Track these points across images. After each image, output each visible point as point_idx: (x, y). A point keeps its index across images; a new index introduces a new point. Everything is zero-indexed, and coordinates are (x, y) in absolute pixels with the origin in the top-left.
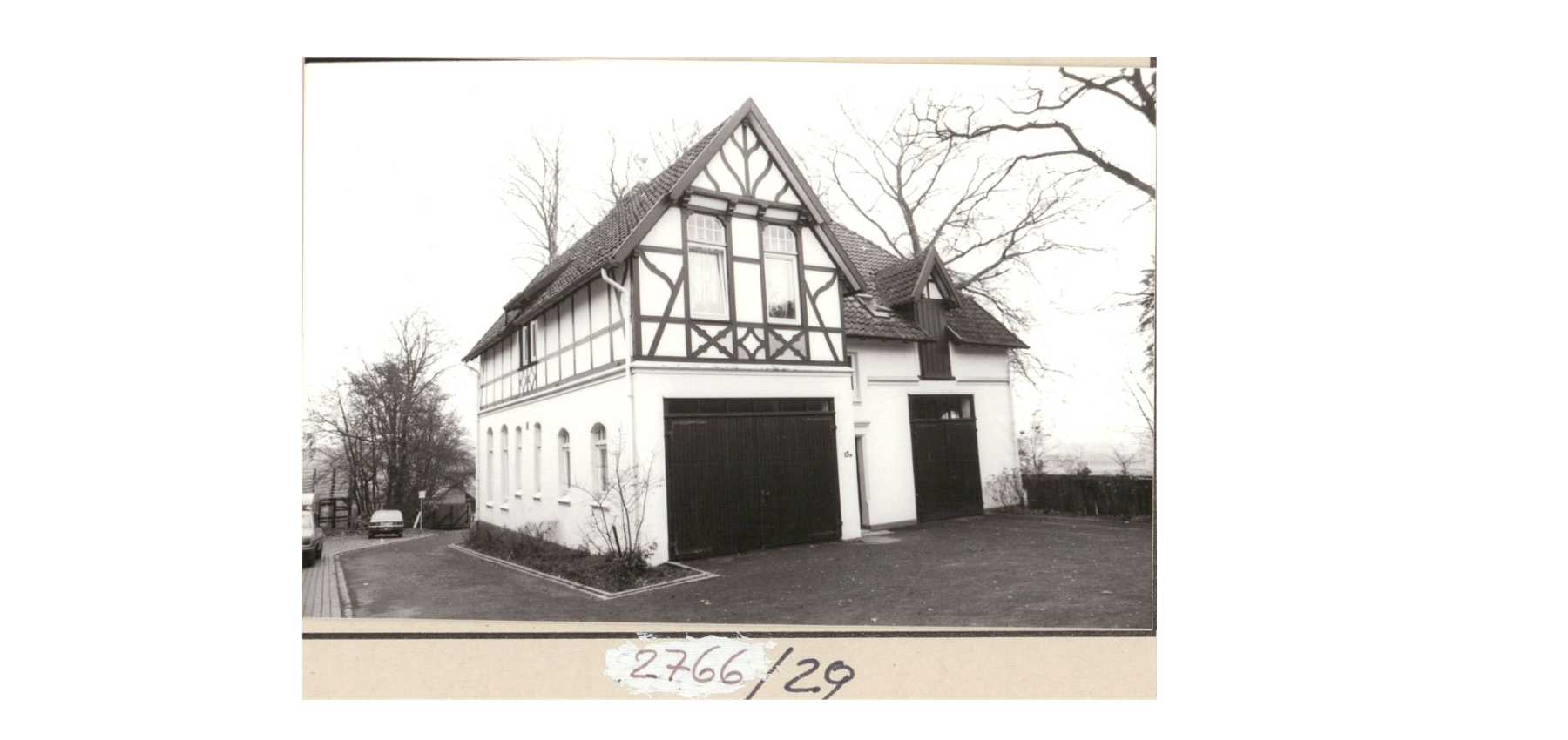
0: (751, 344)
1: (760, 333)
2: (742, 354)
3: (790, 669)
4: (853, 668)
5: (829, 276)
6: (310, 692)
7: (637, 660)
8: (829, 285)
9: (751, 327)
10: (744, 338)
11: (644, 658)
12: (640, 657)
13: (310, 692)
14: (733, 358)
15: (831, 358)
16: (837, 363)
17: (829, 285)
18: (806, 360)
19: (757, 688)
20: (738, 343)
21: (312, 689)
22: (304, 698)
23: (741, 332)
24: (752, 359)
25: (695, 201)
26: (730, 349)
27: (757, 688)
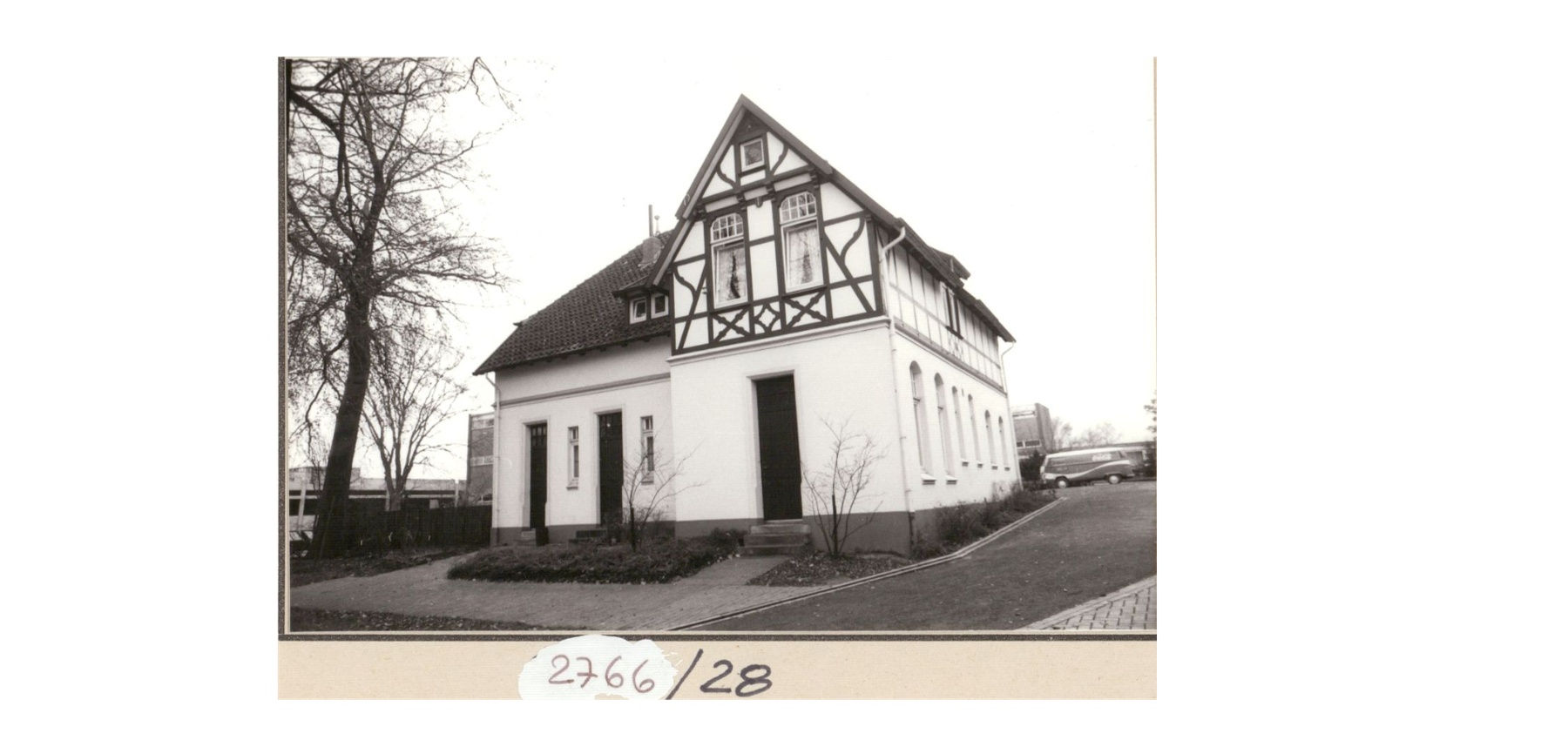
0: (767, 318)
1: (776, 306)
2: (759, 330)
3: (705, 672)
4: (720, 659)
5: (855, 224)
6: (285, 692)
7: (554, 666)
8: (857, 235)
9: (766, 303)
10: (760, 315)
11: (561, 663)
12: (556, 662)
13: (285, 692)
14: (751, 336)
15: (862, 310)
16: (869, 313)
17: (857, 235)
18: (828, 320)
19: (585, 683)
20: (754, 320)
21: (288, 689)
22: (279, 698)
23: (757, 310)
24: (769, 332)
25: (710, 208)
26: (747, 329)
27: (585, 683)
